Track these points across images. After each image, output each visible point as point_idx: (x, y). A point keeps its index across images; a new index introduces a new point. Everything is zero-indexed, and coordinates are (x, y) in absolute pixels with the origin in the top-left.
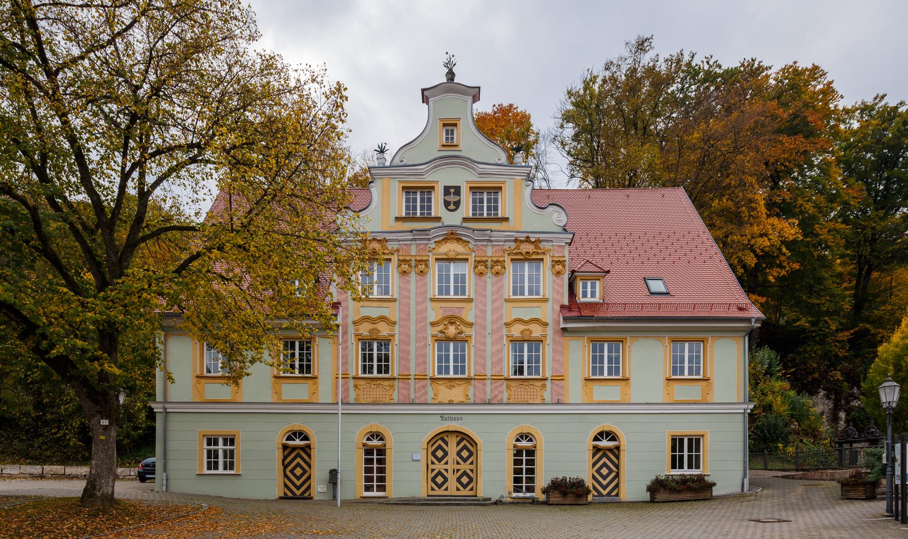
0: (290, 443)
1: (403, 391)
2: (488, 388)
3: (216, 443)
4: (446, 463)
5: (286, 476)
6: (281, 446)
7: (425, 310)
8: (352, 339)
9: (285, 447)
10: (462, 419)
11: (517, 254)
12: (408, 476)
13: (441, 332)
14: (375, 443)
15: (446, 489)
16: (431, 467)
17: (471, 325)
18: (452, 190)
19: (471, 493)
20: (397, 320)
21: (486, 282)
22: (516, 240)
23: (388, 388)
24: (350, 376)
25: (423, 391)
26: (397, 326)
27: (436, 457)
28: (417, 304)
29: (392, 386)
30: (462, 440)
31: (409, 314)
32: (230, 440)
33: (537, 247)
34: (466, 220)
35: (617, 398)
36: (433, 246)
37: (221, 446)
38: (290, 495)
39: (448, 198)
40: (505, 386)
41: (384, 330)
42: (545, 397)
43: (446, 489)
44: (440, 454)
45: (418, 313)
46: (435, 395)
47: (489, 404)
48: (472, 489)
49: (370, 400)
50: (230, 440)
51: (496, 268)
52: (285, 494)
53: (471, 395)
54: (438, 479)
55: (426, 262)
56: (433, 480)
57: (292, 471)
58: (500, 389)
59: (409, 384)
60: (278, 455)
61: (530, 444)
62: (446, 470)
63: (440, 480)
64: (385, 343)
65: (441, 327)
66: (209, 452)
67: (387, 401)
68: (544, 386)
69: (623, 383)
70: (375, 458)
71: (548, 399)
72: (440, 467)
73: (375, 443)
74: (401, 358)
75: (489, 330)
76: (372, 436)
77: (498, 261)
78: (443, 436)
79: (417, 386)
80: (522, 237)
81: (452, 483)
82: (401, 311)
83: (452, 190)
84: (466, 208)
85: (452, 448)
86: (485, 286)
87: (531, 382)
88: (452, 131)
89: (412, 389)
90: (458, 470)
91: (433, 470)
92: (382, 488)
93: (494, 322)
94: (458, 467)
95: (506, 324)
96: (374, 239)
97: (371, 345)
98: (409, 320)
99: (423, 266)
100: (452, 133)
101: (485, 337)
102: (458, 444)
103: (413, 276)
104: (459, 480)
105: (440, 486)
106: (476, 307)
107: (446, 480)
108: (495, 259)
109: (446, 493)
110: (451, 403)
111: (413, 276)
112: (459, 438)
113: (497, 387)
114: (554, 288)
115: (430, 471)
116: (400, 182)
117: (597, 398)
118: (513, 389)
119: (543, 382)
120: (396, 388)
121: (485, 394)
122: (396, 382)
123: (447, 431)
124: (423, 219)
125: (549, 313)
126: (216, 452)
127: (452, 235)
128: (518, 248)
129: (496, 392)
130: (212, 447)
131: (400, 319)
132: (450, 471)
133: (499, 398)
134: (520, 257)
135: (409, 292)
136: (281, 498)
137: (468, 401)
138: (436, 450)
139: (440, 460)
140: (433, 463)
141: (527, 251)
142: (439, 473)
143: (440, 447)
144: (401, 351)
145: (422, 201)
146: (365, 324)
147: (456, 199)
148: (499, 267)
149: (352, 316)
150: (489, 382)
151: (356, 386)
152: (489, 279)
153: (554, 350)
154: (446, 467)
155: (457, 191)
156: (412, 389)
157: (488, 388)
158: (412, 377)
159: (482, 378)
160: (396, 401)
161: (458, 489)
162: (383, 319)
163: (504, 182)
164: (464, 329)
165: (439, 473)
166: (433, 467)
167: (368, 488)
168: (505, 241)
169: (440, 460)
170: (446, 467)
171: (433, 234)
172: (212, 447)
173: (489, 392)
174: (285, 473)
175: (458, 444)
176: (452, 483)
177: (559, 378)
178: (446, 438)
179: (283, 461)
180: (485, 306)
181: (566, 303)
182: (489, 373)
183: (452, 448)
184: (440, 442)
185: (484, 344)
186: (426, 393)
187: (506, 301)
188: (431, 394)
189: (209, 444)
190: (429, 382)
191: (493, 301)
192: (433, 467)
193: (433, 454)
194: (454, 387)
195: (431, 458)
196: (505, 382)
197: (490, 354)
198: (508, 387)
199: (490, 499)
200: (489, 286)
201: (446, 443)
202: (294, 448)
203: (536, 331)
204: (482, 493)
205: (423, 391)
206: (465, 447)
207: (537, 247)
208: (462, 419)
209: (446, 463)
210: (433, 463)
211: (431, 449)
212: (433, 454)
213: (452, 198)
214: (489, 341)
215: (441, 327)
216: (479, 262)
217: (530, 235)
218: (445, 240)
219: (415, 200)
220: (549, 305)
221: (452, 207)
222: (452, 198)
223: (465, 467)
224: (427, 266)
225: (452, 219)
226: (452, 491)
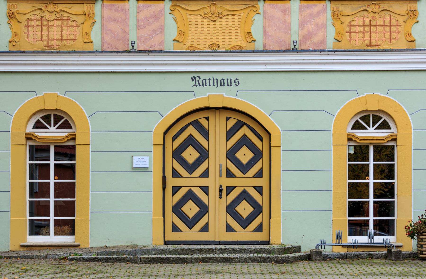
1: (112, 26)
2: (294, 20)
10: (237, 83)
14: (53, 133)
15: (205, 229)
16: (172, 182)
23: (80, 19)
25: (155, 25)
27: (183, 163)
29: (90, 15)
30: (239, 125)
40: (329, 13)
43: (205, 229)
46: (181, 33)
47: (295, 51)
48: (259, 229)
54: (185, 208)
58: (320, 20)
59: (126, 12)
62: (205, 190)
63: (191, 209)
67: (79, 45)
72: (190, 182)
73: (53, 133)
78: (195, 118)
79: (142, 15)
81: (217, 216)
85: (218, 145)
89: (132, 22)
90: (230, 189)
91: (176, 190)
92: (69, 227)
94: (231, 182)
102: (230, 134)
104: (231, 209)
107: (204, 210)
110: (214, 50)
112: (232, 122)
113: (312, 16)
115: (169, 190)
118: (347, 20)
120: (98, 18)
121: (288, 30)
129: (311, 27)
132: (214, 191)
133: (316, 39)
140: (176, 174)
142: (190, 196)
143: (190, 141)
154: (204, 182)
156: (132, 22)
157: (294, 20)
161: (229, 229)
166: (177, 182)
167: (37, 228)
170: (204, 182)
175: (230, 134)
176: (217, 216)
178: (204, 122)
183: (218, 145)
184: (191, 131)
186: (162, 28)
188: (172, 31)
192: (177, 182)
193: (177, 154)
194: (220, 16)
199: (298, 249)
205: (155, 25)
206: (245, 142)
208: (237, 83)
209: (205, 174)
210: (176, 174)
212: (177, 154)
223: (244, 182)
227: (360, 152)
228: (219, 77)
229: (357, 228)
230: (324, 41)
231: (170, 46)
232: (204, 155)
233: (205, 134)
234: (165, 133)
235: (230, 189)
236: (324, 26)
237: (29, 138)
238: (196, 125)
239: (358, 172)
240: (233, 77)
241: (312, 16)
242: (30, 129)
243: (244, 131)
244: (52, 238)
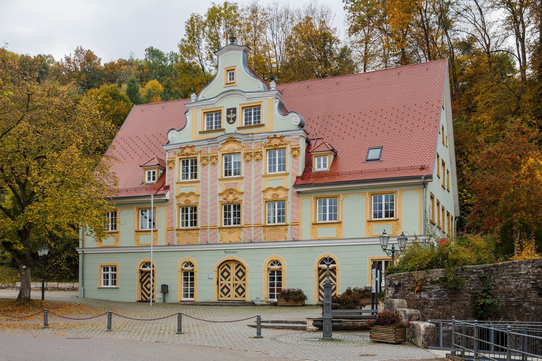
0: (144, 269)
1: (203, 237)
2: (253, 233)
3: (108, 271)
4: (229, 280)
5: (142, 288)
6: (139, 271)
7: (216, 186)
8: (175, 207)
9: (142, 272)
10: (237, 252)
11: (269, 146)
12: (206, 289)
13: (225, 199)
15: (229, 296)
16: (220, 282)
17: (242, 193)
18: (231, 111)
19: (243, 299)
20: (200, 194)
21: (251, 166)
23: (195, 235)
24: (175, 229)
25: (215, 236)
26: (200, 197)
28: (212, 183)
29: (197, 234)
31: (206, 189)
32: (114, 269)
33: (282, 141)
34: (239, 128)
35: (334, 235)
36: (220, 146)
37: (110, 272)
38: (144, 299)
41: (193, 200)
42: (287, 236)
44: (226, 274)
45: (212, 188)
46: (222, 238)
47: (251, 242)
49: (185, 243)
51: (257, 156)
52: (142, 299)
53: (242, 238)
54: (224, 290)
55: (216, 157)
56: (222, 290)
57: (145, 286)
58: (259, 233)
59: (207, 232)
60: (138, 276)
61: (279, 267)
62: (229, 284)
63: (225, 290)
64: (194, 209)
65: (225, 196)
66: (104, 275)
67: (195, 243)
68: (286, 230)
69: (338, 225)
70: (189, 276)
71: (289, 238)
72: (225, 282)
74: (202, 217)
75: (253, 196)
76: (274, 263)
77: (257, 152)
78: (226, 263)
79: (211, 233)
80: (272, 135)
81: (233, 293)
82: (202, 188)
83: (231, 111)
84: (240, 120)
85: (233, 271)
86: (251, 168)
87: (278, 227)
88: (233, 73)
89: (209, 235)
90: (236, 284)
91: (221, 284)
93: (256, 190)
94: (236, 282)
95: (263, 191)
96: (187, 146)
97: (187, 209)
98: (207, 193)
99: (215, 160)
100: (233, 75)
101: (250, 200)
102: (236, 268)
103: (209, 166)
105: (225, 294)
106: (246, 182)
107: (229, 291)
108: (256, 151)
109: (229, 299)
110: (230, 243)
111: (209, 166)
112: (237, 264)
113: (257, 231)
114: (292, 166)
115: (220, 285)
116: (202, 110)
117: (320, 236)
118: (267, 232)
119: (285, 227)
121: (251, 236)
122: (200, 231)
123: (228, 260)
124: (216, 131)
125: (288, 182)
126: (108, 275)
127: (231, 139)
128: (270, 142)
129: (257, 235)
130: (106, 272)
131: (202, 193)
132: (232, 285)
133: (258, 238)
134: (272, 148)
135: (207, 176)
136: (139, 301)
137: (197, 243)
138: (223, 272)
139: (226, 278)
140: (221, 280)
141: (276, 145)
142: (225, 286)
143: (226, 270)
144: (203, 212)
145: (216, 118)
146: (182, 197)
147: (234, 115)
148: (259, 156)
149: (176, 194)
150: (253, 229)
151: (178, 235)
152: (253, 163)
153: (293, 206)
154: (229, 282)
155: (234, 110)
156: (209, 235)
157: (253, 233)
158: (209, 228)
159: (248, 226)
160: (199, 243)
161: (236, 296)
162: (192, 193)
163: (262, 102)
164: (238, 196)
165: (225, 286)
166: (222, 282)
168: (262, 139)
169: (226, 278)
170: (229, 282)
171: (219, 139)
172: (106, 272)
173: (253, 235)
175: (236, 268)
176: (233, 293)
177: (296, 224)
178: (229, 264)
179: (141, 280)
180: (251, 181)
181: (300, 174)
182: (253, 223)
183: (233, 271)
184: (226, 267)
185: (250, 205)
186: (216, 237)
187: (264, 176)
188: (219, 238)
189: (104, 271)
190: (218, 230)
191: (256, 177)
192: (222, 282)
193: (222, 274)
194: (232, 232)
195: (221, 277)
196: (262, 228)
197: (254, 211)
198: (264, 231)
200: (253, 168)
201: (229, 268)
203: (281, 195)
204: (248, 299)
205: (215, 236)
206: (240, 270)
207: (282, 141)
208: (237, 252)
210: (221, 280)
211: (220, 272)
212: (222, 274)
213: (231, 116)
214: (253, 202)
215: (225, 196)
216: (247, 153)
217: (276, 134)
219: (212, 119)
220: (290, 176)
221: (231, 121)
222: (231, 116)
223: (240, 282)
224: (217, 159)
225: (230, 129)
226: (233, 298)
227: (273, 272)
228: (232, 251)
229: (272, 296)
230: (261, 239)
231: (219, 242)
232: (229, 274)
233: (229, 268)
234: (219, 267)
235: (236, 284)
236: (261, 234)
237: (182, 270)
238: (227, 265)
239: (272, 279)
240: (235, 251)
241: (257, 231)
242: (183, 267)
243: (240, 267)
244: (189, 299)
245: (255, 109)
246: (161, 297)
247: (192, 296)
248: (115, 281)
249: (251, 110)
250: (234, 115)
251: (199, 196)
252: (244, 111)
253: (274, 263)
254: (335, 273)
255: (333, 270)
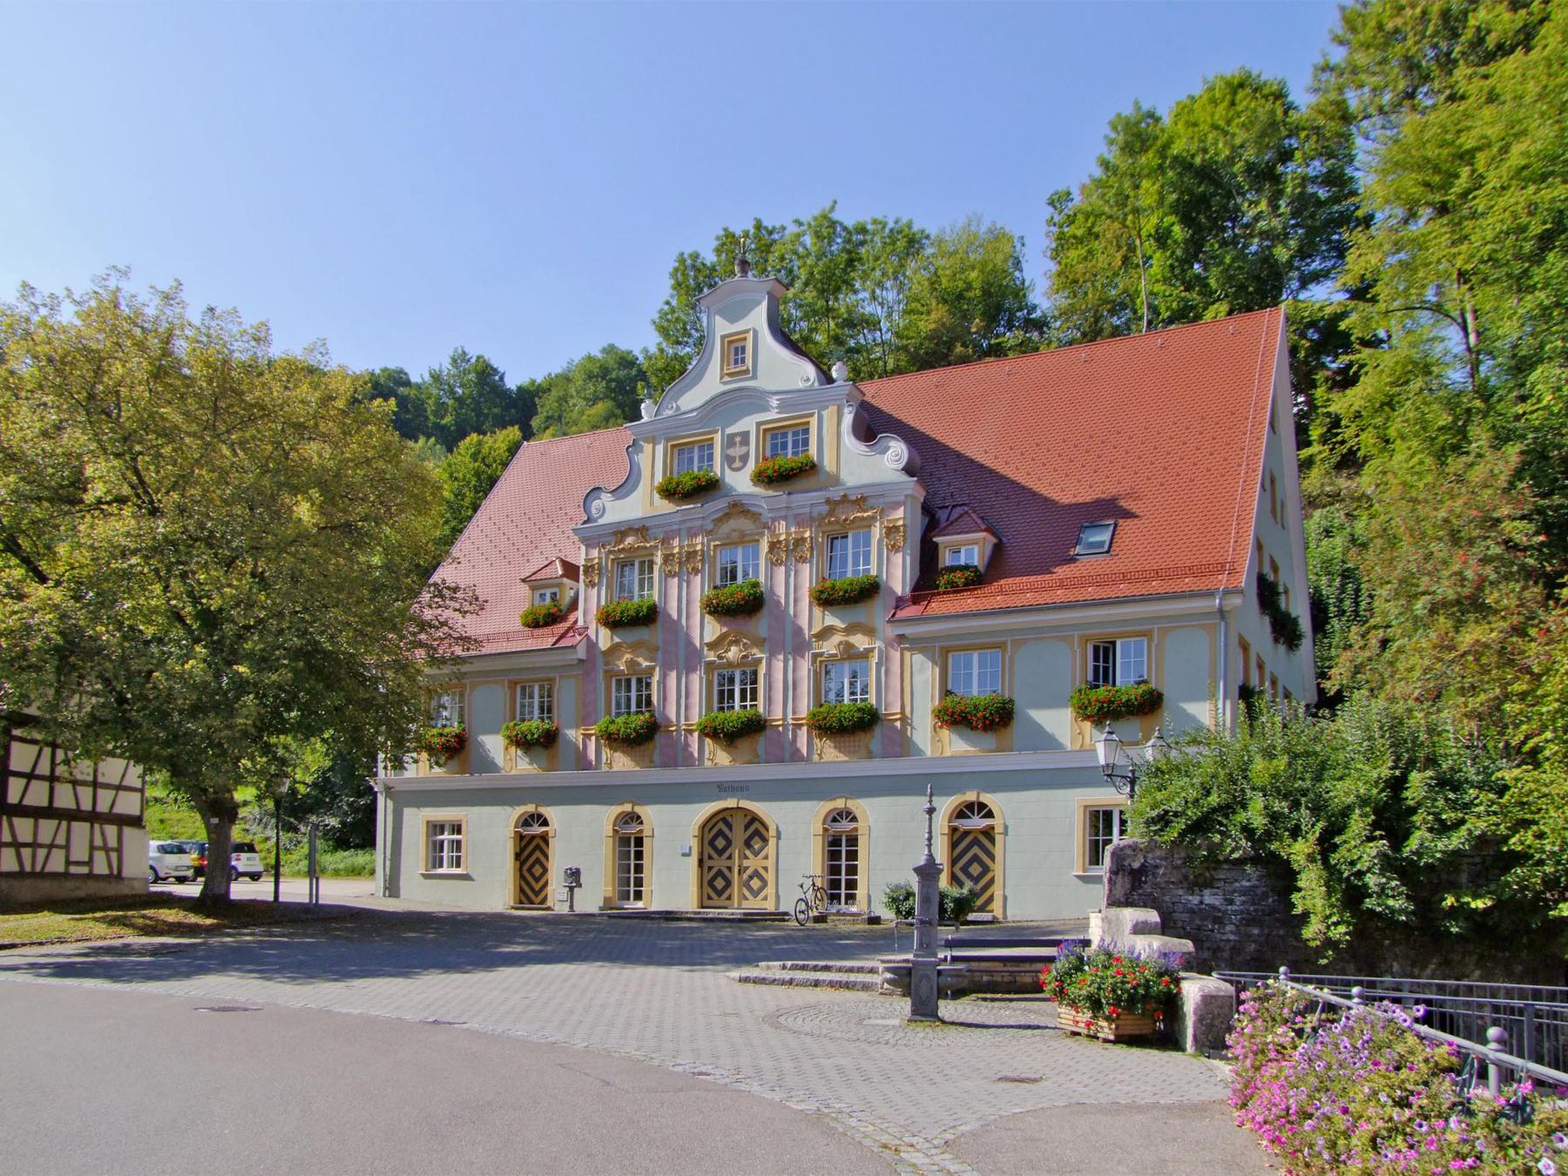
5: (522, 877)
16: (708, 863)
18: (738, 439)
22: (828, 501)
27: (715, 848)
39: (731, 452)
50: (457, 829)
57: (529, 870)
78: (722, 817)
83: (738, 439)
85: (738, 835)
91: (710, 868)
97: (628, 682)
102: (747, 827)
140: (710, 858)
142: (720, 873)
143: (720, 833)
147: (743, 450)
154: (729, 863)
166: (711, 863)
170: (729, 863)
174: (521, 870)
175: (747, 827)
184: (721, 825)
192: (711, 863)
193: (712, 843)
195: (708, 850)
201: (730, 827)
202: (533, 837)
210: (710, 858)
212: (712, 843)
218: (727, 516)
221: (737, 464)
227: (835, 842)
232: (729, 843)
238: (724, 820)
243: (757, 825)
245: (795, 434)
246: (565, 897)
247: (638, 896)
248: (459, 858)
249: (785, 435)
250: (743, 450)
251: (657, 649)
252: (768, 437)
253: (840, 814)
254: (992, 841)
255: (988, 833)
